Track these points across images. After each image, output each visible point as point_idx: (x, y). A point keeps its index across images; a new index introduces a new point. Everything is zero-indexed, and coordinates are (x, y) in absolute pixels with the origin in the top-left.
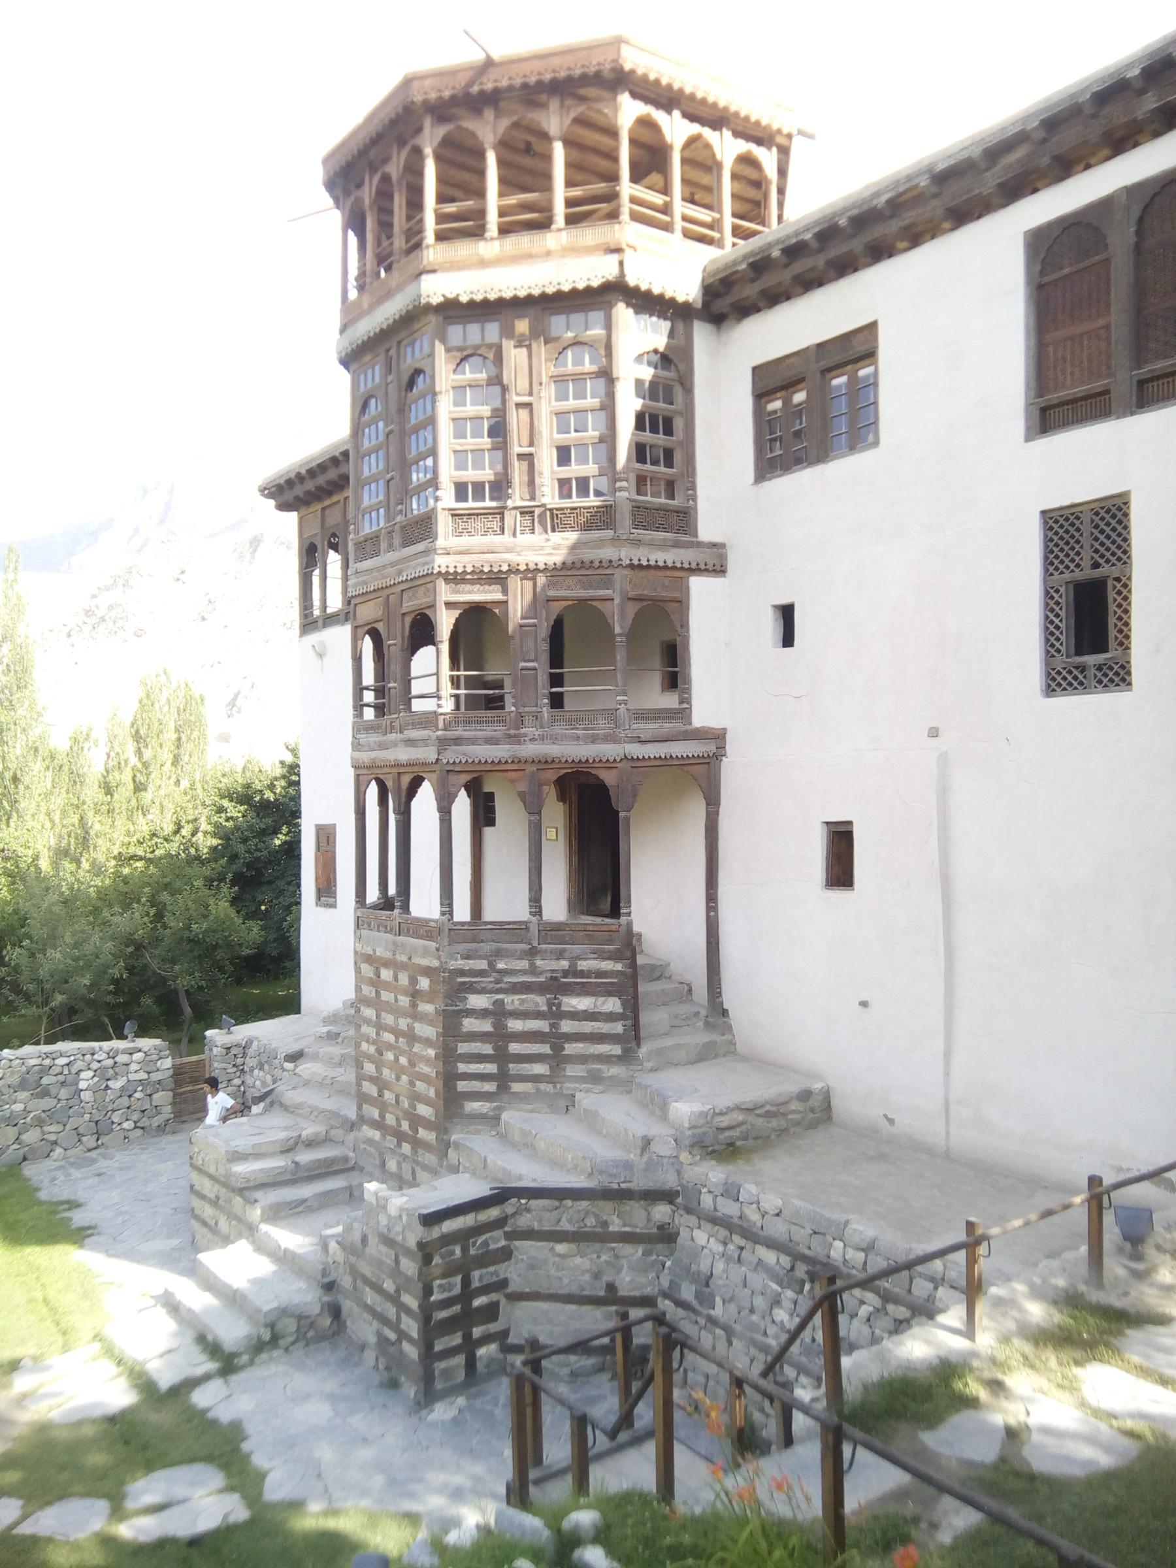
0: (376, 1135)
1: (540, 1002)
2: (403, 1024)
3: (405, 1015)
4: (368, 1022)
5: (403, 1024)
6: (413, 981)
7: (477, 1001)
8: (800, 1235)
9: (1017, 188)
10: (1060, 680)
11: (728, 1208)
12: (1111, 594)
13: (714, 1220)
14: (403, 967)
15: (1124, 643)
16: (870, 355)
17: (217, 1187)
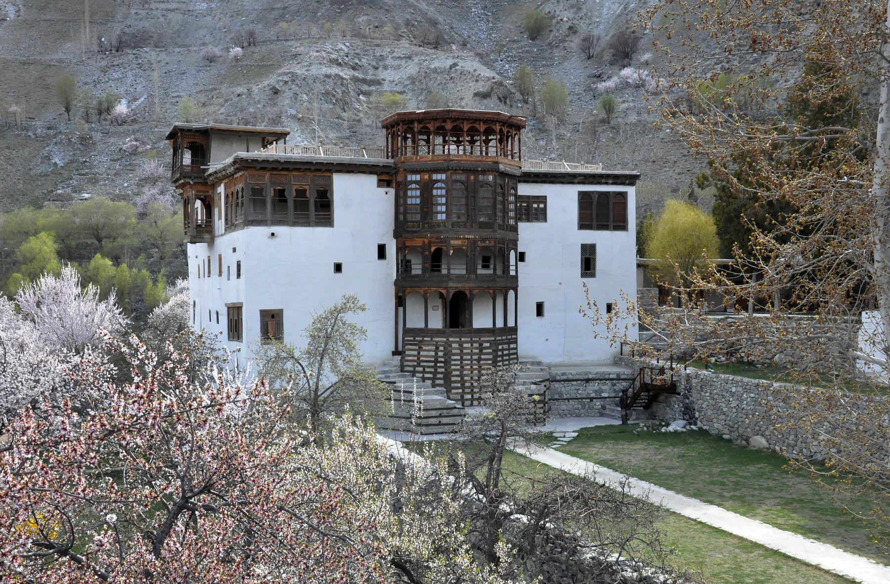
0: (460, 391)
1: (506, 346)
2: (474, 357)
3: (476, 354)
4: (455, 360)
5: (474, 357)
6: (481, 345)
7: (500, 347)
8: (582, 377)
9: (579, 183)
10: (584, 275)
11: (565, 377)
12: (592, 262)
13: (560, 381)
14: (476, 342)
15: (594, 269)
16: (545, 203)
17: (440, 412)
